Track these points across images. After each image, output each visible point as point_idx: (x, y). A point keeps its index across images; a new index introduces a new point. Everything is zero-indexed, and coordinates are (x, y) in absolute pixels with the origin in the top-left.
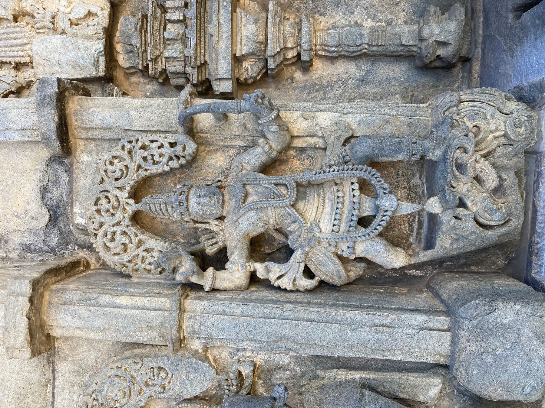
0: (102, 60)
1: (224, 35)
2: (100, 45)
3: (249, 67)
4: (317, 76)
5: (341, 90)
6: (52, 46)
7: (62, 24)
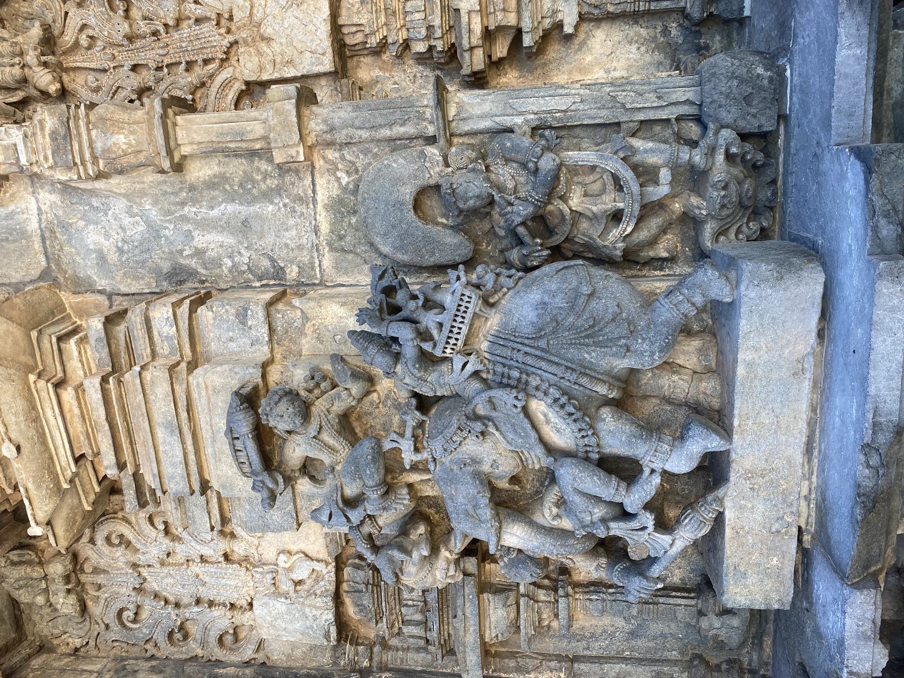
1: (472, 629)
2: (330, 616)
4: (578, 626)
6: (276, 611)
7: (286, 586)
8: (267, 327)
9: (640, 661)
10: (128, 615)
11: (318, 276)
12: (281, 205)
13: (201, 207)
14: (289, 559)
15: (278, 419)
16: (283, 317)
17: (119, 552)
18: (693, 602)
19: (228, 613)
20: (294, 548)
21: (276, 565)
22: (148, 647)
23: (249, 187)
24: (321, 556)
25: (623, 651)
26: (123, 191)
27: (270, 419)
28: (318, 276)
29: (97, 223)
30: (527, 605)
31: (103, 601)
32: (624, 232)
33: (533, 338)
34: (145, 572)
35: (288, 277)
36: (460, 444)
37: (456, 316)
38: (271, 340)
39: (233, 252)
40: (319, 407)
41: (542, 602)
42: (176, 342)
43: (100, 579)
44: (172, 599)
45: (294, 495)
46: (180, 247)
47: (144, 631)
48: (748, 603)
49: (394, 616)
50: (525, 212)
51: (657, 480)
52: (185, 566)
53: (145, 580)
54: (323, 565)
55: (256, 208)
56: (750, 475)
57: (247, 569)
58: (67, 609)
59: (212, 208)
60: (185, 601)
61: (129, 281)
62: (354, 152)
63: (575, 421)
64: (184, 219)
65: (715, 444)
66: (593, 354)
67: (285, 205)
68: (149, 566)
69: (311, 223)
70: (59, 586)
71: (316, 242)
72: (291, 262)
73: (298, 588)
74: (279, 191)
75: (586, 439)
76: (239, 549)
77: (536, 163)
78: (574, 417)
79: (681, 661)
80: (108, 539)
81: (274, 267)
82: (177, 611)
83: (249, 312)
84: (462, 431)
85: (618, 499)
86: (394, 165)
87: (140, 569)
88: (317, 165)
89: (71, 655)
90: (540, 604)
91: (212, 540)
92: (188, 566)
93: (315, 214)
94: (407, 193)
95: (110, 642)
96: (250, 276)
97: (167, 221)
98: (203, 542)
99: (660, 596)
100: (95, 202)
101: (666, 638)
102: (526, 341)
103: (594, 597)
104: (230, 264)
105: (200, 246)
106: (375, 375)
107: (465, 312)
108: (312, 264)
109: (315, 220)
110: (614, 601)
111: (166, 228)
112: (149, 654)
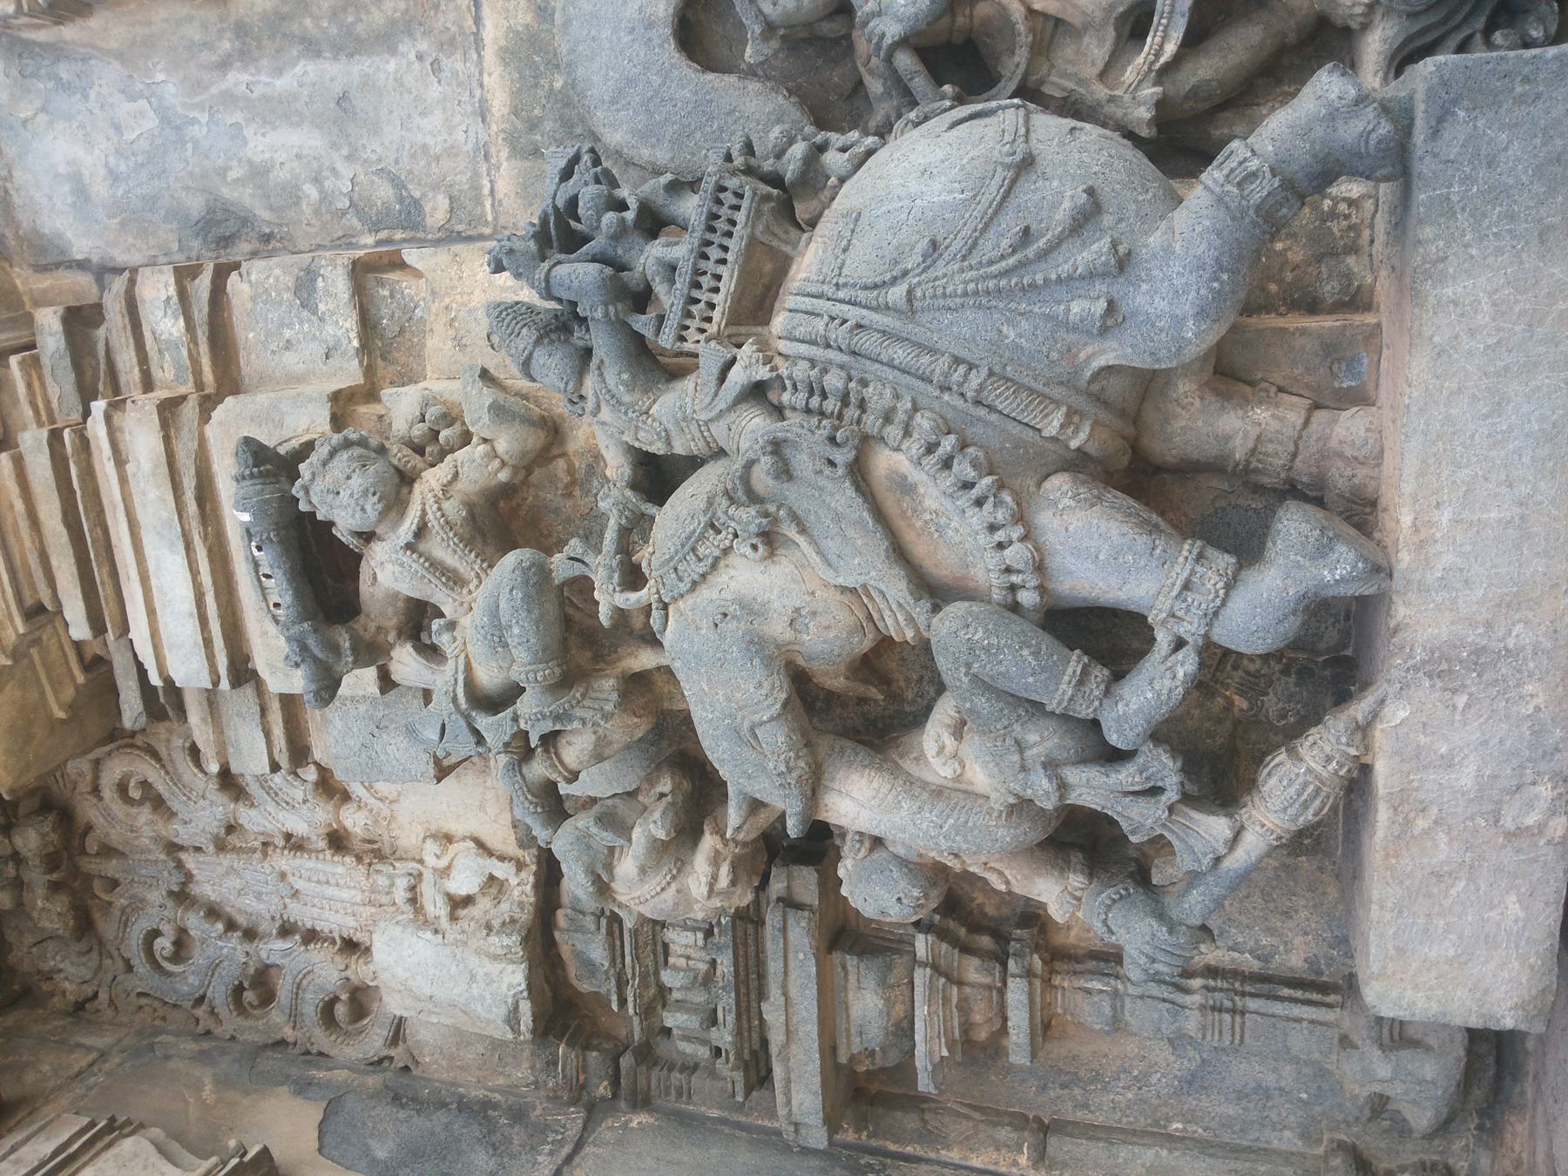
0: (526, 1008)
2: (515, 977)
5: (1130, 1096)
9: (1206, 1147)
10: (164, 945)
11: (490, 218)
12: (412, 56)
13: (259, 71)
16: (392, 296)
17: (144, 815)
19: (338, 959)
21: (421, 861)
22: (200, 1012)
23: (350, 19)
25: (1169, 1120)
26: (114, 45)
28: (490, 218)
29: (70, 119)
30: (931, 987)
31: (118, 913)
32: (1158, 55)
33: (876, 286)
34: (190, 861)
35: (429, 221)
36: (714, 566)
37: (709, 243)
38: (365, 347)
39: (320, 171)
41: (973, 985)
42: (185, 352)
43: (112, 867)
44: (241, 920)
47: (191, 979)
48: (1434, 1008)
51: (1186, 664)
52: (258, 855)
53: (189, 877)
55: (361, 66)
56: (1443, 668)
58: (52, 921)
59: (279, 72)
60: (264, 927)
61: (130, 240)
63: (979, 503)
64: (229, 99)
65: (1338, 570)
66: (1025, 325)
67: (420, 57)
68: (198, 849)
69: (472, 95)
70: (36, 876)
71: (483, 137)
72: (435, 187)
73: (462, 913)
75: (1007, 552)
76: (353, 820)
78: (975, 492)
79: (1303, 1156)
80: (122, 788)
81: (401, 200)
82: (247, 947)
83: (320, 283)
84: (718, 532)
85: (1084, 711)
87: (183, 856)
89: (68, 1014)
90: (968, 990)
91: (305, 801)
92: (265, 854)
93: (481, 74)
95: (133, 995)
96: (355, 221)
97: (195, 106)
98: (289, 805)
99: (1252, 995)
100: (65, 71)
101: (1268, 1098)
102: (862, 296)
103: (1096, 985)
105: (257, 159)
107: (729, 234)
108: (476, 187)
109: (482, 86)
110: (1141, 997)
111: (194, 121)
112: (200, 1029)
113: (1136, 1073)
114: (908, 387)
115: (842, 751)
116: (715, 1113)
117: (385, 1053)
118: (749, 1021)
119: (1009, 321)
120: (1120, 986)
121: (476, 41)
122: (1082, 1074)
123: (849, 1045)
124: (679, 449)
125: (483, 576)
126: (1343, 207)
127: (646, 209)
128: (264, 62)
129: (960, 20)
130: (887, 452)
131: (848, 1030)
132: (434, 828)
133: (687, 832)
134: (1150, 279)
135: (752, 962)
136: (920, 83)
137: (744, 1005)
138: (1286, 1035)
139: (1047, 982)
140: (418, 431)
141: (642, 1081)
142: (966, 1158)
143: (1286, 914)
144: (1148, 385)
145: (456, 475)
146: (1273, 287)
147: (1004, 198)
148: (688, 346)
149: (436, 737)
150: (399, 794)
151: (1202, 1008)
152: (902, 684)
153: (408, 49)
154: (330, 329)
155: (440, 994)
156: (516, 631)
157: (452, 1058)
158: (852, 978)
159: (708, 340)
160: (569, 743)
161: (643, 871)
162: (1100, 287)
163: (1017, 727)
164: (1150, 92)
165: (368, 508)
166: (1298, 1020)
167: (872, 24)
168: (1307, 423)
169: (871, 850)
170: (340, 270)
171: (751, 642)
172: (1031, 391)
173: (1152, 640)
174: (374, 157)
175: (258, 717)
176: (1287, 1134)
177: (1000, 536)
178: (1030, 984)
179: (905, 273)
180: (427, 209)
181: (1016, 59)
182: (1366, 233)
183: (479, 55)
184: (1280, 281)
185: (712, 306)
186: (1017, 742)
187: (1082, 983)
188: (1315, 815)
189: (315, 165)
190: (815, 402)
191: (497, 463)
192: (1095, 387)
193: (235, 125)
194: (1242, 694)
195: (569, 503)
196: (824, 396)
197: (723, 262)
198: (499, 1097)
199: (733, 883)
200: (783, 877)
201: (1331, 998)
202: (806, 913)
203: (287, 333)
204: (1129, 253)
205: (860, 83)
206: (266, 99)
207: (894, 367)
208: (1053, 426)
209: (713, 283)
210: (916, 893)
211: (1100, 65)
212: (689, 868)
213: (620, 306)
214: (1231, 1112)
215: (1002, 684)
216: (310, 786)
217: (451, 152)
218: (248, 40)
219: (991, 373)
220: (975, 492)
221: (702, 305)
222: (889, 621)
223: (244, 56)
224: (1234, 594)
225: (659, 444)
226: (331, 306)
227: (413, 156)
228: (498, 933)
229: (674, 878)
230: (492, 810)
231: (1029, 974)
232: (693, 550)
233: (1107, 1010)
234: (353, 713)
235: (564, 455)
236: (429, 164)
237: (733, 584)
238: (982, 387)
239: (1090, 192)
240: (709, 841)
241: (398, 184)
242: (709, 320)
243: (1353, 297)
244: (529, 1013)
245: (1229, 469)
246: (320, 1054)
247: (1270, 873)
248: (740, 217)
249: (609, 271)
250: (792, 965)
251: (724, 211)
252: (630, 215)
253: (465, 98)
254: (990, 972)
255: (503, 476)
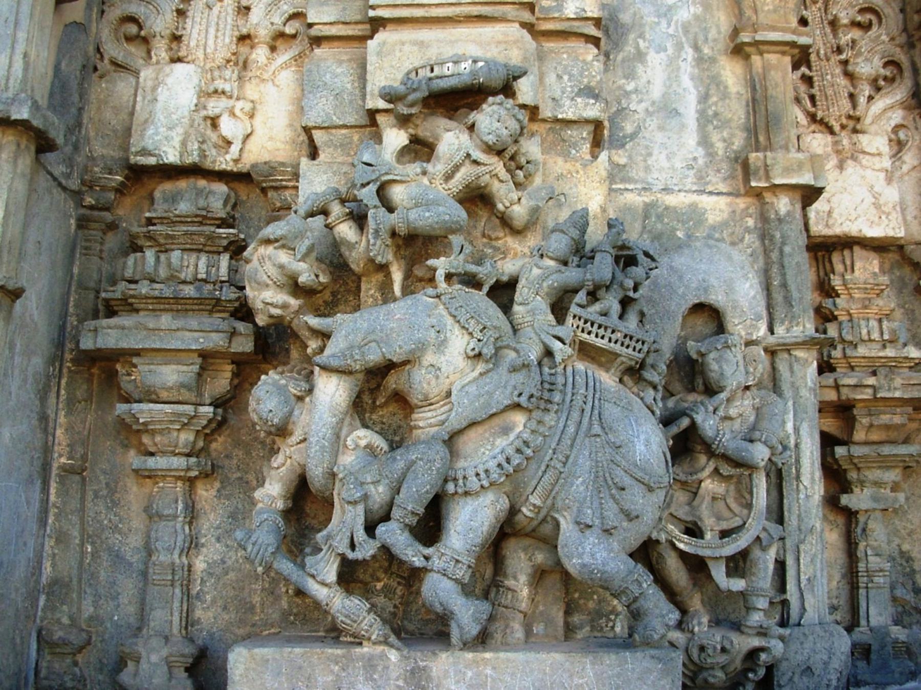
0: (152, 161)
2: (172, 157)
3: (133, 378)
4: (129, 485)
5: (105, 522)
7: (215, 106)
8: (574, 118)
11: (614, 186)
13: (693, 67)
14: (246, 114)
15: (496, 116)
18: (175, 630)
19: (168, 32)
20: (258, 121)
21: (238, 99)
23: (715, 123)
24: (245, 155)
27: (495, 107)
28: (614, 186)
32: (679, 540)
33: (600, 419)
35: (613, 152)
38: (557, 120)
39: (641, 93)
40: (498, 166)
42: (556, 15)
45: (352, 127)
46: (647, 36)
49: (162, 241)
50: (707, 427)
51: (418, 562)
54: (236, 156)
57: (228, 61)
62: (753, 242)
64: (679, 47)
66: (582, 488)
67: (695, 159)
69: (675, 185)
73: (209, 122)
74: (711, 155)
75: (475, 479)
77: (760, 440)
78: (505, 465)
81: (625, 137)
83: (592, 101)
84: (481, 331)
85: (396, 513)
86: (748, 285)
88: (738, 200)
91: (272, 24)
93: (686, 191)
94: (717, 298)
102: (596, 412)
103: (180, 506)
104: (630, 87)
105: (649, 58)
106: (526, 236)
107: (622, 345)
109: (679, 191)
110: (176, 531)
111: (669, 25)
113: (120, 526)
114: (555, 433)
115: (357, 386)
116: (76, 270)
117: (106, 57)
118: (152, 303)
119: (584, 481)
120: (180, 519)
121: (701, 191)
122: (117, 495)
123: (143, 364)
124: (516, 308)
125: (449, 192)
126: (611, 624)
127: (633, 300)
128: (696, 71)
129: (699, 447)
130: (523, 421)
131: (152, 364)
132: (258, 106)
133: (296, 288)
134: (599, 544)
135: (188, 307)
136: (675, 430)
137: (163, 301)
138: (163, 608)
139: (179, 478)
140: (523, 160)
141: (96, 225)
142: (61, 426)
143: (225, 608)
144: (550, 543)
145: (502, 181)
146: (576, 595)
147: (636, 479)
148: (570, 320)
149: (365, 159)
150: (278, 86)
151: (173, 564)
152: (381, 413)
153: (700, 152)
154: (568, 103)
155: (159, 105)
156: (427, 214)
157: (106, 103)
158: (185, 368)
159: (574, 331)
160: (350, 228)
161: (281, 267)
162: (597, 522)
163: (387, 481)
164: (663, 537)
165: (491, 136)
166: (172, 615)
167: (702, 408)
168: (521, 612)
169: (295, 395)
170: (598, 114)
171: (424, 344)
172: (551, 491)
173: (429, 547)
174: (647, 125)
175: (343, 20)
176: (92, 609)
177: (483, 475)
178: (182, 470)
179: (606, 434)
180: (620, 152)
181: (681, 474)
182: (599, 635)
183: (694, 191)
184: (579, 598)
185: (589, 333)
186: (379, 481)
187: (180, 499)
188: (342, 621)
189: (644, 91)
190: (547, 386)
191: (508, 204)
192: (549, 519)
193: (666, 50)
194: (385, 586)
195: (479, 235)
196: (550, 390)
197: (610, 341)
198: (83, 132)
199: (271, 316)
200: (247, 332)
201: (184, 632)
202: (226, 345)
203: (566, 77)
204: (611, 534)
205: (672, 395)
206: (679, 69)
207: (565, 427)
208: (535, 500)
209: (600, 335)
210: (276, 421)
211: (675, 514)
212: (278, 290)
213: (591, 287)
214: (101, 578)
215: (410, 476)
216: (281, 28)
217: (647, 169)
218: (708, 64)
219: (561, 473)
220: (505, 465)
221: (590, 329)
222: (429, 414)
223: (700, 60)
224: (453, 582)
225: (520, 299)
226: (579, 105)
227: (647, 147)
228: (200, 148)
229: (275, 283)
230: (270, 145)
231: (188, 469)
232: (472, 317)
233: (166, 512)
234: (346, 80)
235: (505, 235)
236: (642, 155)
237: (454, 337)
238: (555, 468)
239: (637, 517)
240: (294, 303)
241: (633, 136)
242: (583, 331)
243: (571, 630)
244: (148, 163)
245: (498, 578)
246: (103, 12)
247: (248, 600)
248: (630, 351)
249: (608, 283)
250: (196, 334)
251: (633, 343)
252: (631, 294)
253: (674, 181)
254: (185, 446)
255: (500, 207)
